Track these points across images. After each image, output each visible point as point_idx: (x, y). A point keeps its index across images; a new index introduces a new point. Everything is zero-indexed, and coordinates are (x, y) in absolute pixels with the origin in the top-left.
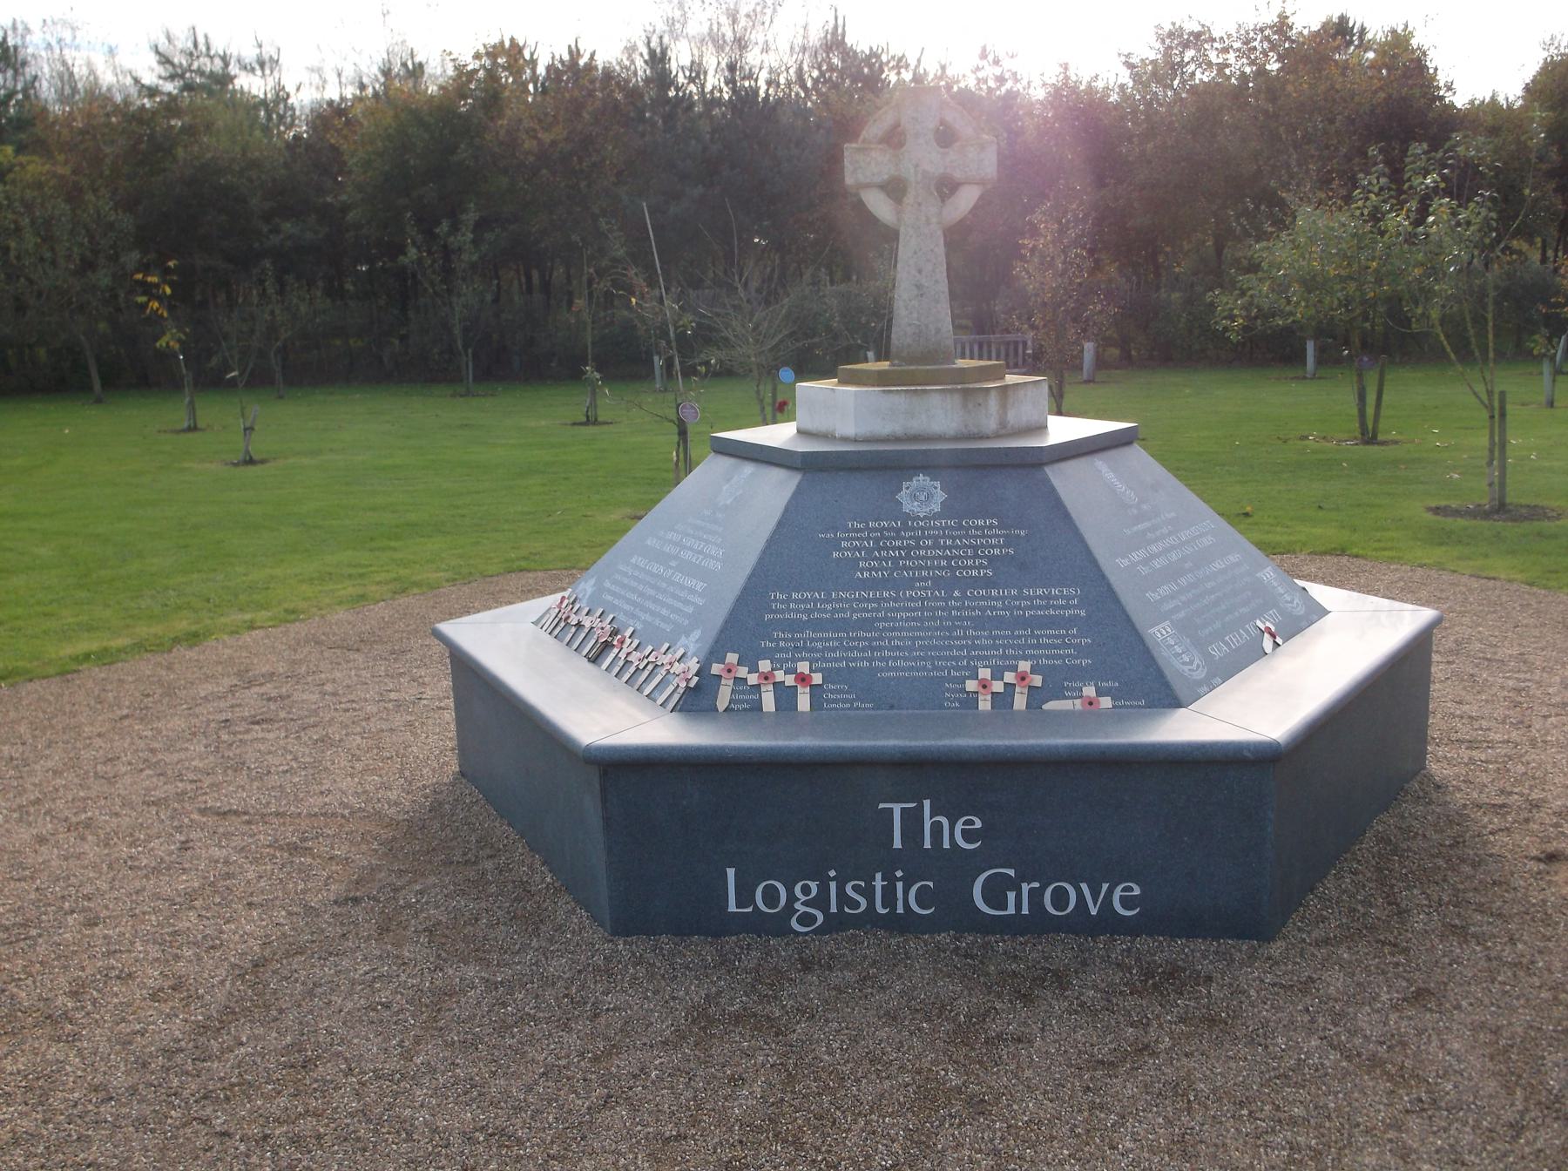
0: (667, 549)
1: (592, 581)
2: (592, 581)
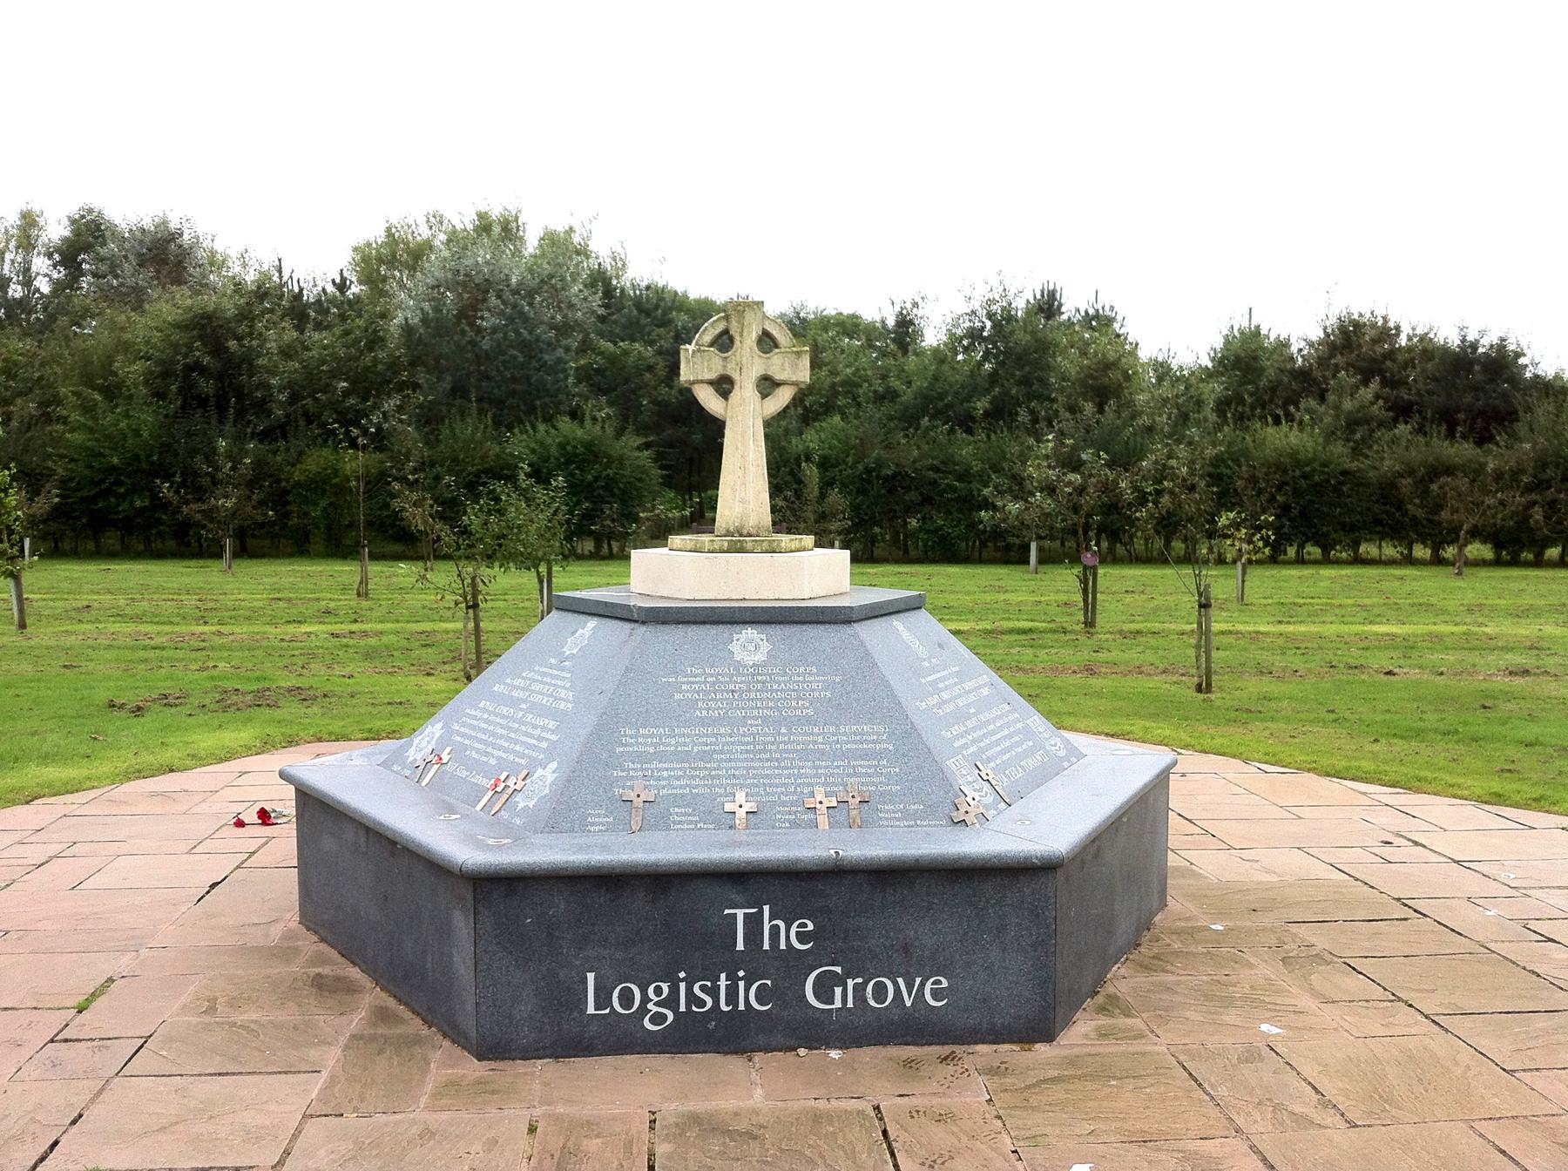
0: (515, 694)
1: (440, 725)
2: (440, 725)
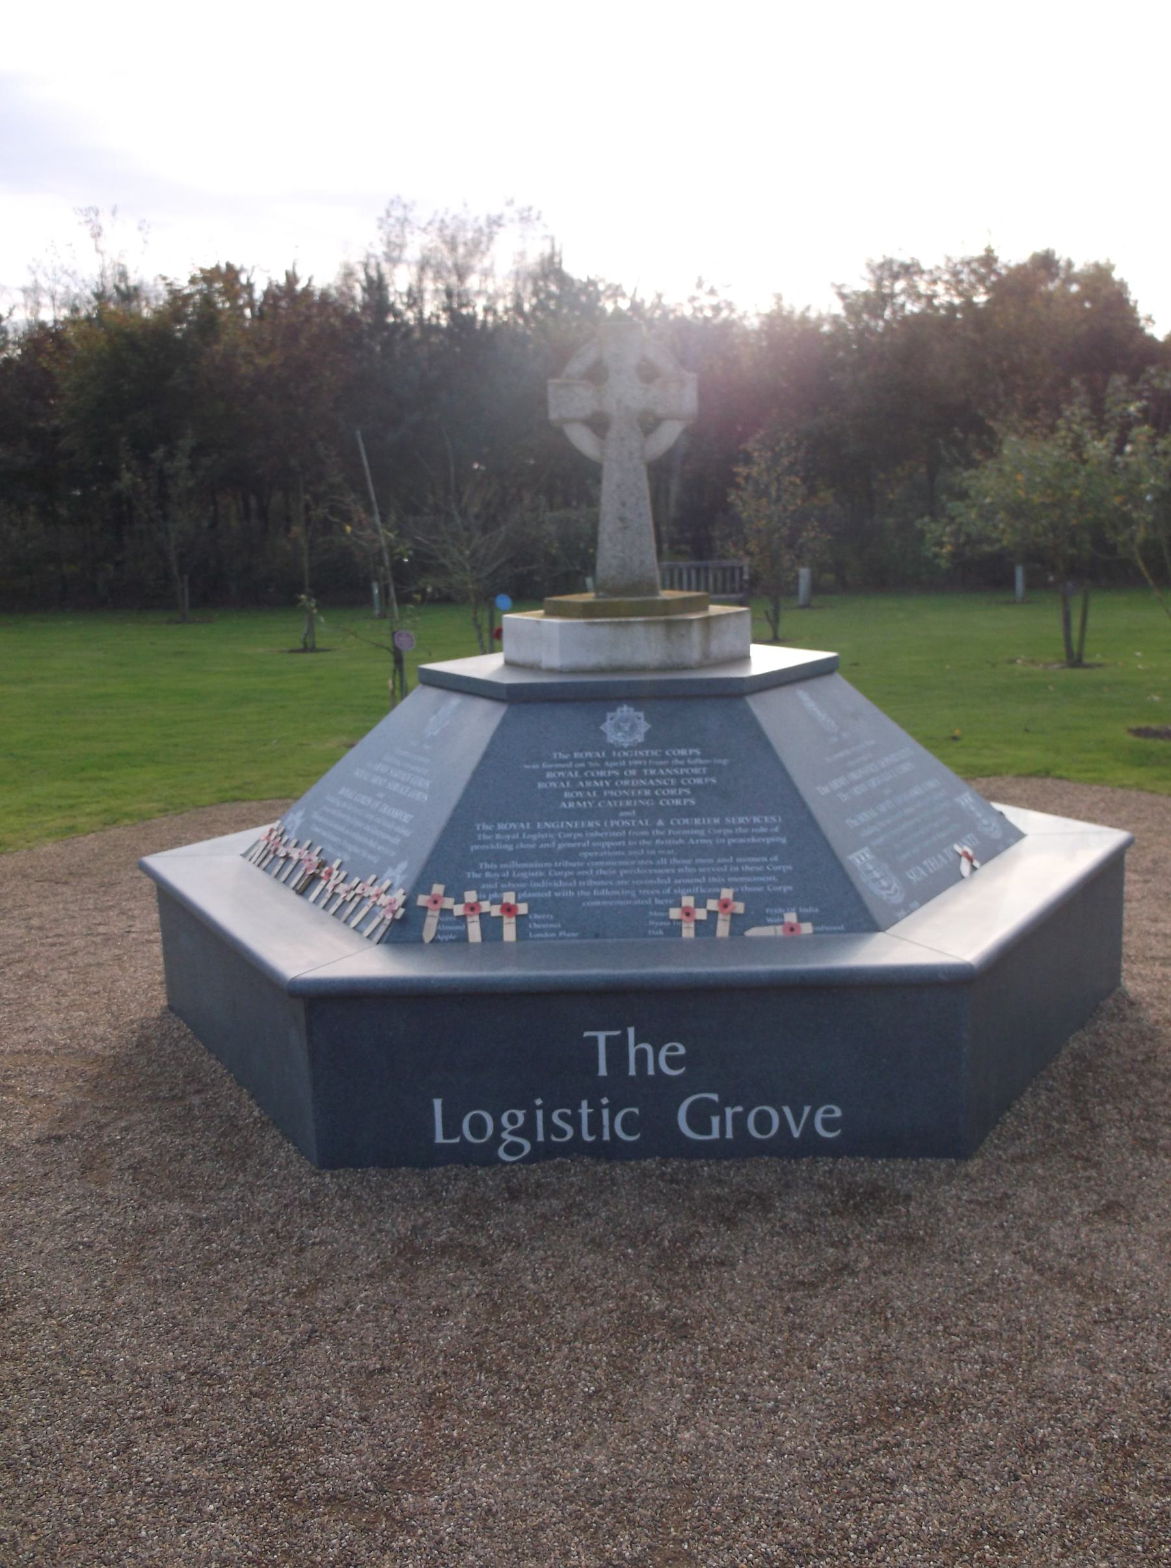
0: (375, 780)
1: (300, 814)
2: (300, 814)
